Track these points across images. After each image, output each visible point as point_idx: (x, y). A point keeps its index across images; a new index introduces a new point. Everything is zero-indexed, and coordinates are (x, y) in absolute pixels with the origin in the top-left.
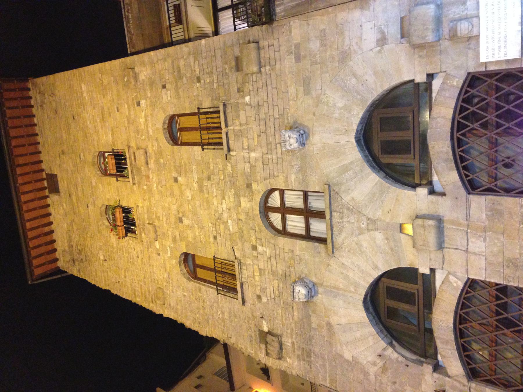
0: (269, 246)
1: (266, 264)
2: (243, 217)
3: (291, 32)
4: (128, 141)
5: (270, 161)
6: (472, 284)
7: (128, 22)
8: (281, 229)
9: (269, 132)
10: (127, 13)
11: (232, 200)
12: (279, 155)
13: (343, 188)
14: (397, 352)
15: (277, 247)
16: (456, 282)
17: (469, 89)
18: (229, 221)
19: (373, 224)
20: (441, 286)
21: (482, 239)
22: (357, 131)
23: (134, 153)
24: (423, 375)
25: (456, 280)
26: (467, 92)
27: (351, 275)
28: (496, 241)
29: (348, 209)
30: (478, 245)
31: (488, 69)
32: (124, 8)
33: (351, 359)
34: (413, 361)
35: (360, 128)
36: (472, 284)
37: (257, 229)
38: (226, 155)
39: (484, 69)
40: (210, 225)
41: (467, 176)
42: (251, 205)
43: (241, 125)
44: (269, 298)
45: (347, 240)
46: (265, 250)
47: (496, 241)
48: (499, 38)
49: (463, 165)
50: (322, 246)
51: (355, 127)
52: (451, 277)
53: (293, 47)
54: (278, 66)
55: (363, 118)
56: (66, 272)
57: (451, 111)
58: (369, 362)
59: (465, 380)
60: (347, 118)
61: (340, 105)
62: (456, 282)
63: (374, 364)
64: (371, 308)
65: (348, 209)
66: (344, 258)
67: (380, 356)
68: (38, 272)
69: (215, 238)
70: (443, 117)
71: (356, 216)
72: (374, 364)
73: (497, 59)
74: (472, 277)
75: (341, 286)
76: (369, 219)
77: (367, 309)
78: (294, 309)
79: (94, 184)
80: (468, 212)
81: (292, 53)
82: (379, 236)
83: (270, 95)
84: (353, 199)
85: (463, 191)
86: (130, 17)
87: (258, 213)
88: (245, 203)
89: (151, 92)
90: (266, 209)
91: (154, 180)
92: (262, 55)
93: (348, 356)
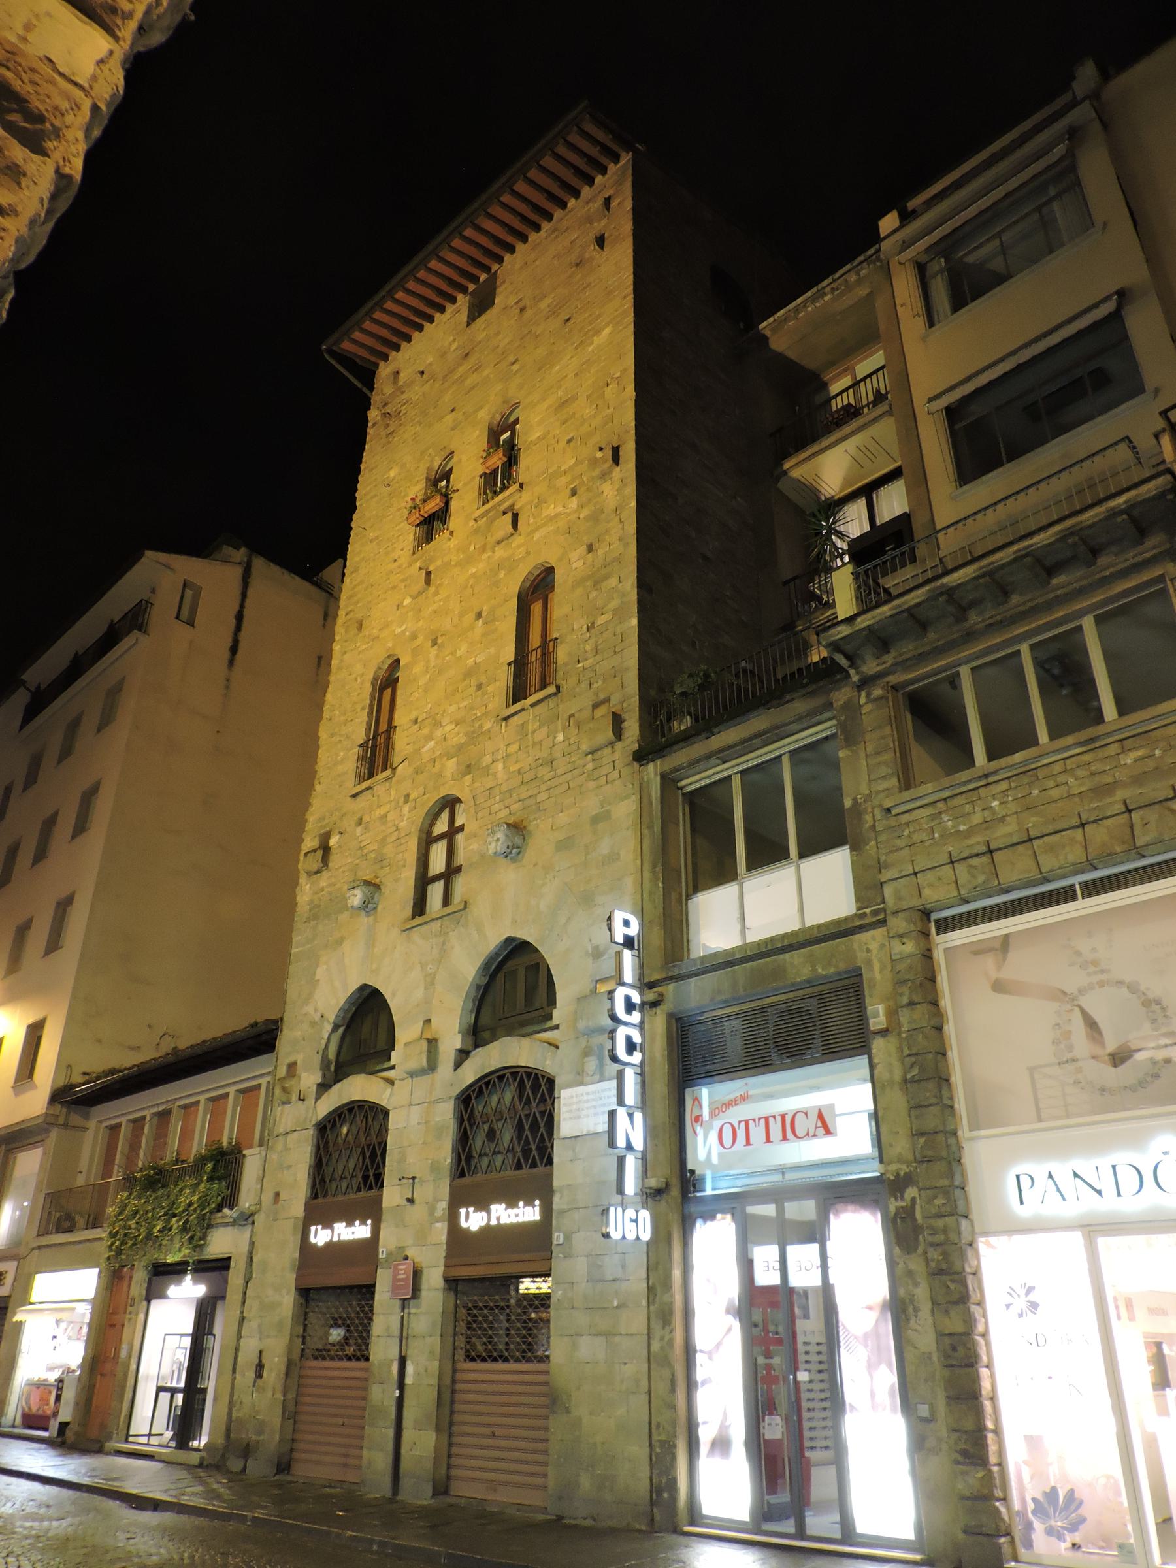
0: (409, 820)
7: (814, 299)
9: (524, 788)
10: (827, 290)
19: (430, 982)
26: (543, 1077)
29: (444, 943)
30: (416, 1114)
32: (834, 281)
56: (372, 389)
63: (316, 1010)
65: (444, 943)
68: (346, 345)
69: (416, 721)
72: (316, 1010)
86: (827, 298)
93: (319, 971)
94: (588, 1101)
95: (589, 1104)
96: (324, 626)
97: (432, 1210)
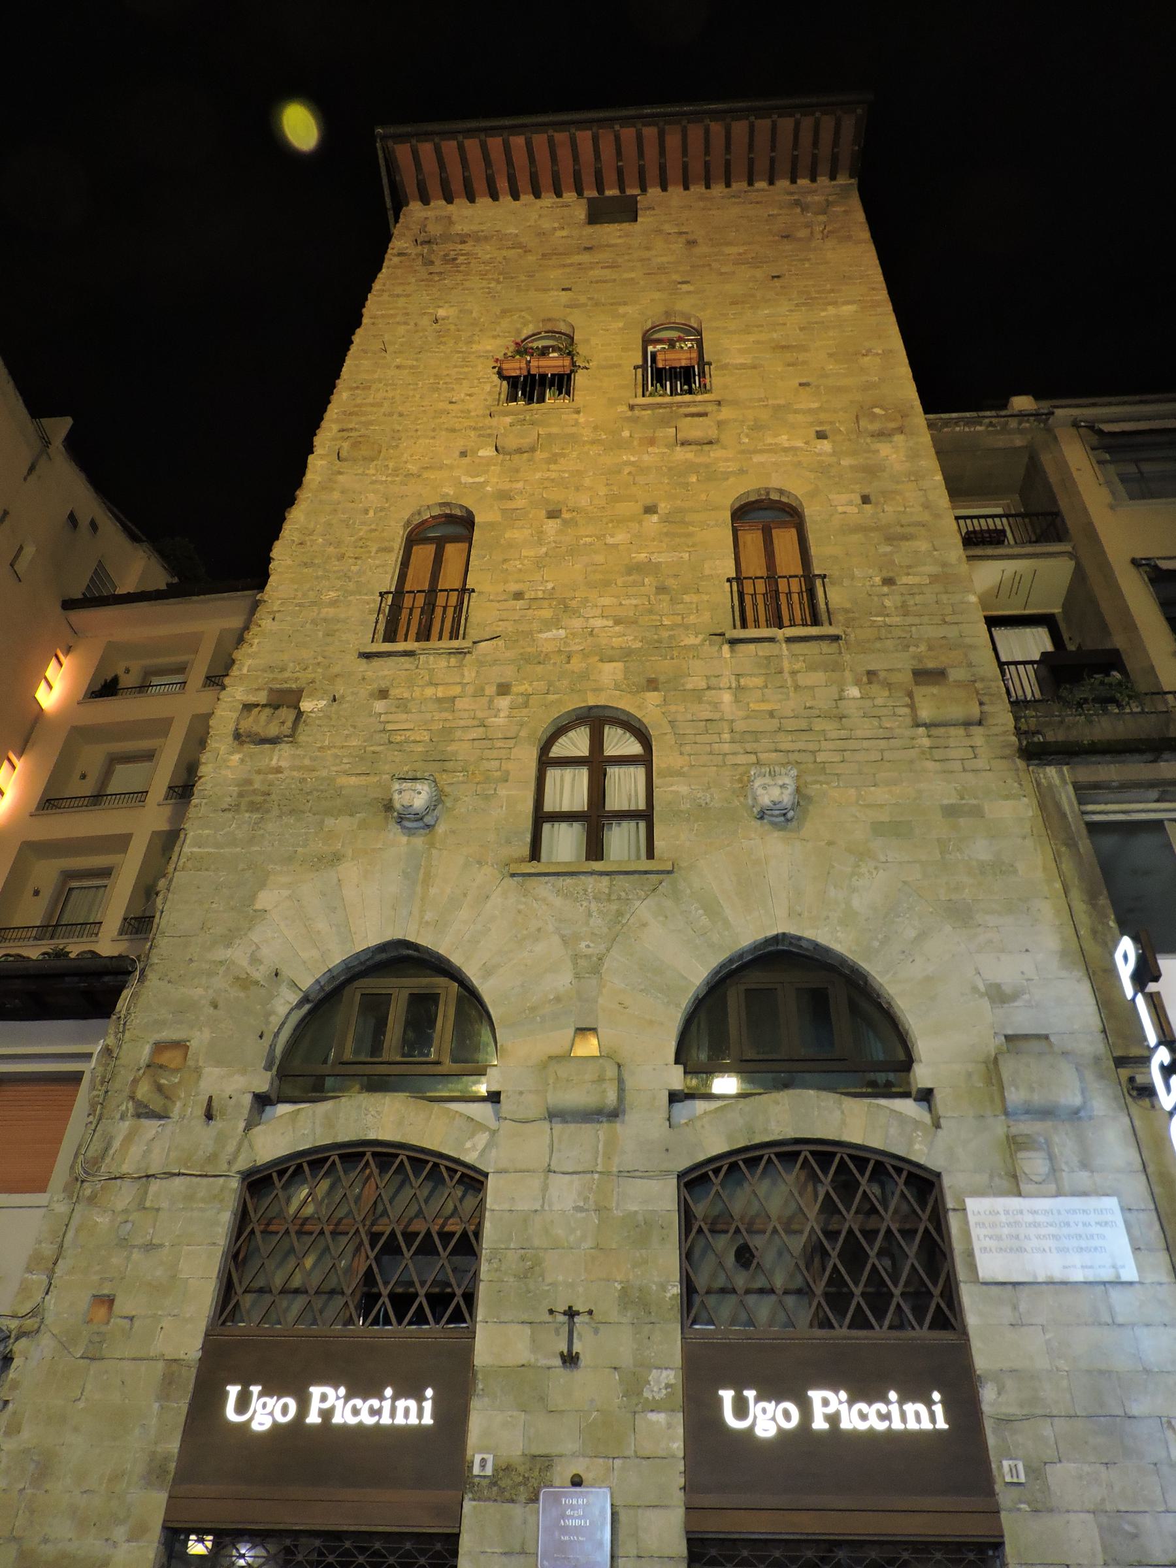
0: (515, 725)
1: (466, 715)
2: (576, 664)
3: (1007, 797)
4: (735, 403)
5: (716, 738)
6: (473, 1181)
7: (969, 422)
8: (551, 755)
9: (781, 737)
10: (987, 421)
11: (616, 642)
12: (731, 760)
13: (668, 903)
14: (289, 1013)
15: (511, 743)
16: (474, 1148)
17: (905, 1174)
18: (562, 632)
19: (590, 969)
20: (461, 1115)
21: (582, 1204)
22: (800, 938)
23: (705, 414)
24: (243, 1072)
25: (480, 1147)
26: (899, 1171)
27: (464, 913)
28: (578, 1233)
29: (620, 914)
30: (565, 1194)
31: (951, 1214)
32: (998, 416)
33: (258, 906)
34: (272, 1048)
35: (804, 944)
36: (473, 1181)
37: (551, 697)
38: (722, 634)
39: (950, 1205)
40: (550, 586)
41: (717, 1171)
42: (608, 686)
43: (793, 673)
44: (383, 718)
45: (544, 907)
46: (502, 714)
47: (578, 1233)
48: (1017, 1237)
49: (741, 1163)
50: (526, 851)
51: (809, 933)
52: (482, 1139)
53: (974, 802)
54: (930, 765)
55: (827, 950)
56: (397, 221)
57: (857, 1139)
58: (258, 947)
59: (243, 1164)
60: (828, 917)
61: (856, 903)
62: (474, 1148)
63: (255, 960)
64: (384, 956)
65: (620, 914)
66: (504, 899)
67: (277, 975)
68: (402, 152)
69: (518, 596)
70: (843, 1123)
71: (605, 930)
73: (975, 1232)
74: (491, 1183)
75: (433, 891)
76: (600, 959)
77: (383, 948)
78: (363, 778)
79: (621, 310)
80: (637, 1174)
81: (962, 798)
82: (564, 980)
83: (866, 744)
84: (645, 925)
85: (684, 1164)
86: (979, 428)
87: (591, 703)
88: (611, 672)
89: (851, 467)
90: (596, 720)
91: (646, 457)
92: (953, 731)
93: (265, 899)
94: (1036, 1225)
95: (1043, 1231)
96: (25, 479)
97: (633, 1384)
